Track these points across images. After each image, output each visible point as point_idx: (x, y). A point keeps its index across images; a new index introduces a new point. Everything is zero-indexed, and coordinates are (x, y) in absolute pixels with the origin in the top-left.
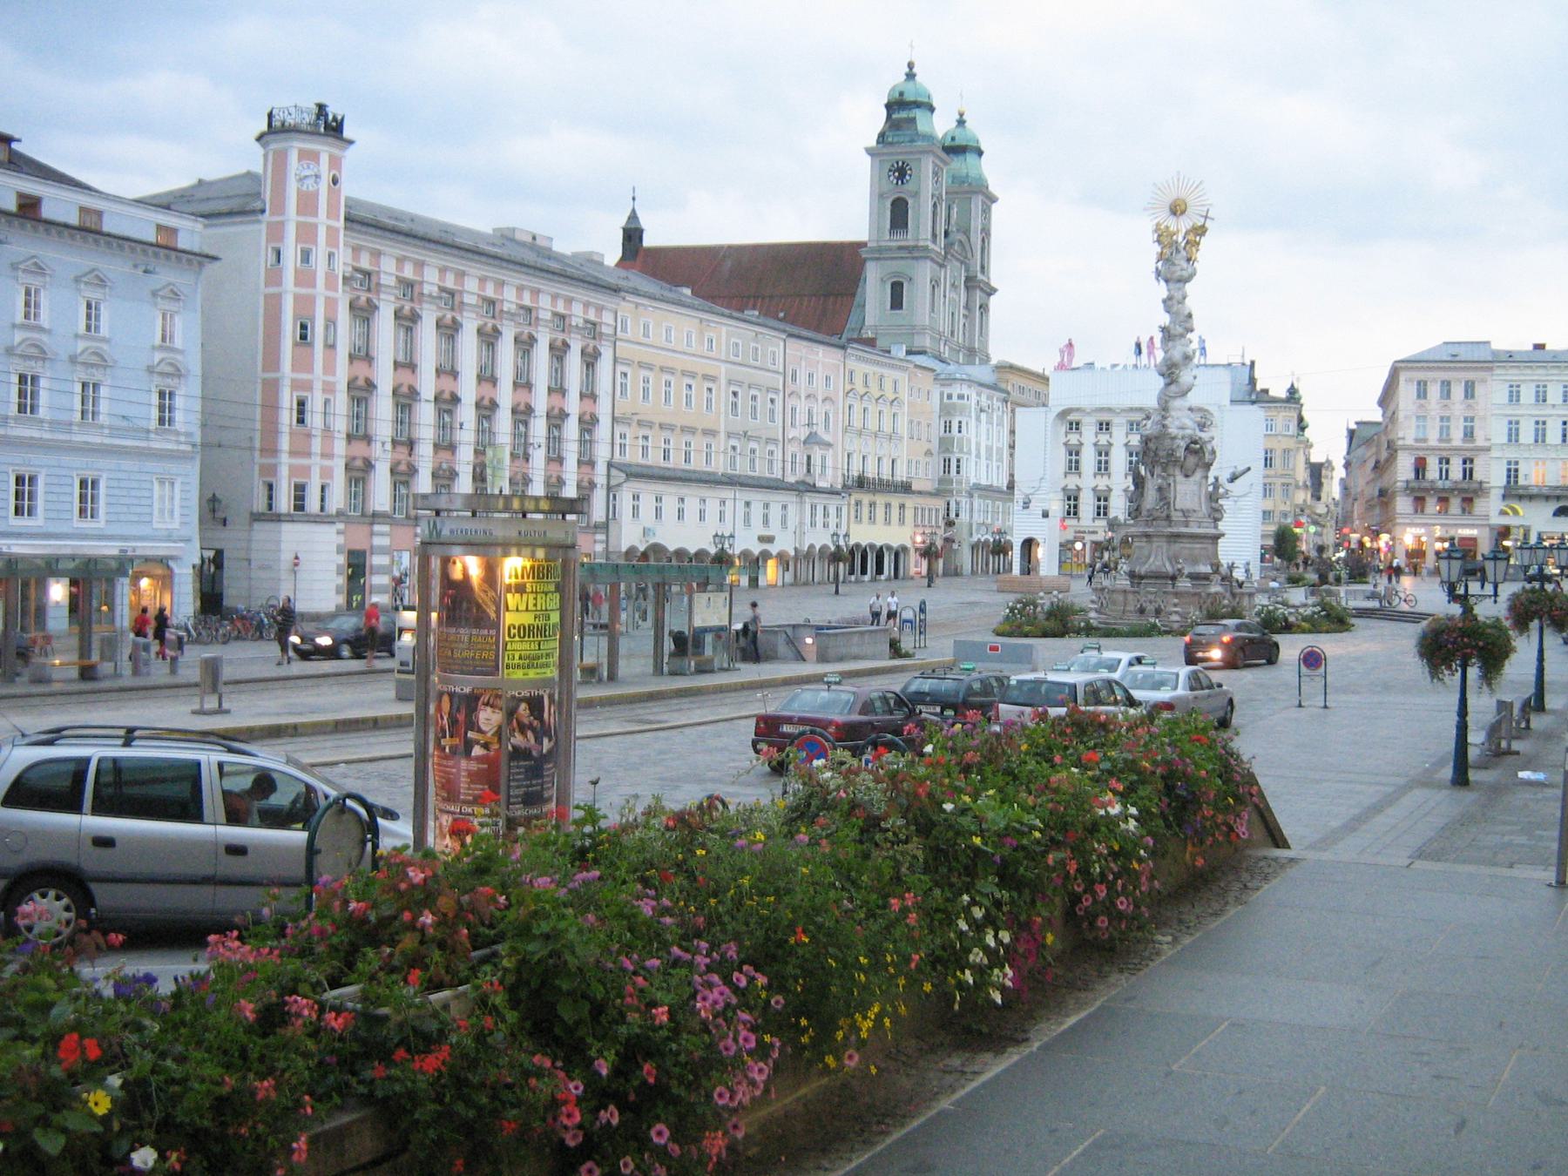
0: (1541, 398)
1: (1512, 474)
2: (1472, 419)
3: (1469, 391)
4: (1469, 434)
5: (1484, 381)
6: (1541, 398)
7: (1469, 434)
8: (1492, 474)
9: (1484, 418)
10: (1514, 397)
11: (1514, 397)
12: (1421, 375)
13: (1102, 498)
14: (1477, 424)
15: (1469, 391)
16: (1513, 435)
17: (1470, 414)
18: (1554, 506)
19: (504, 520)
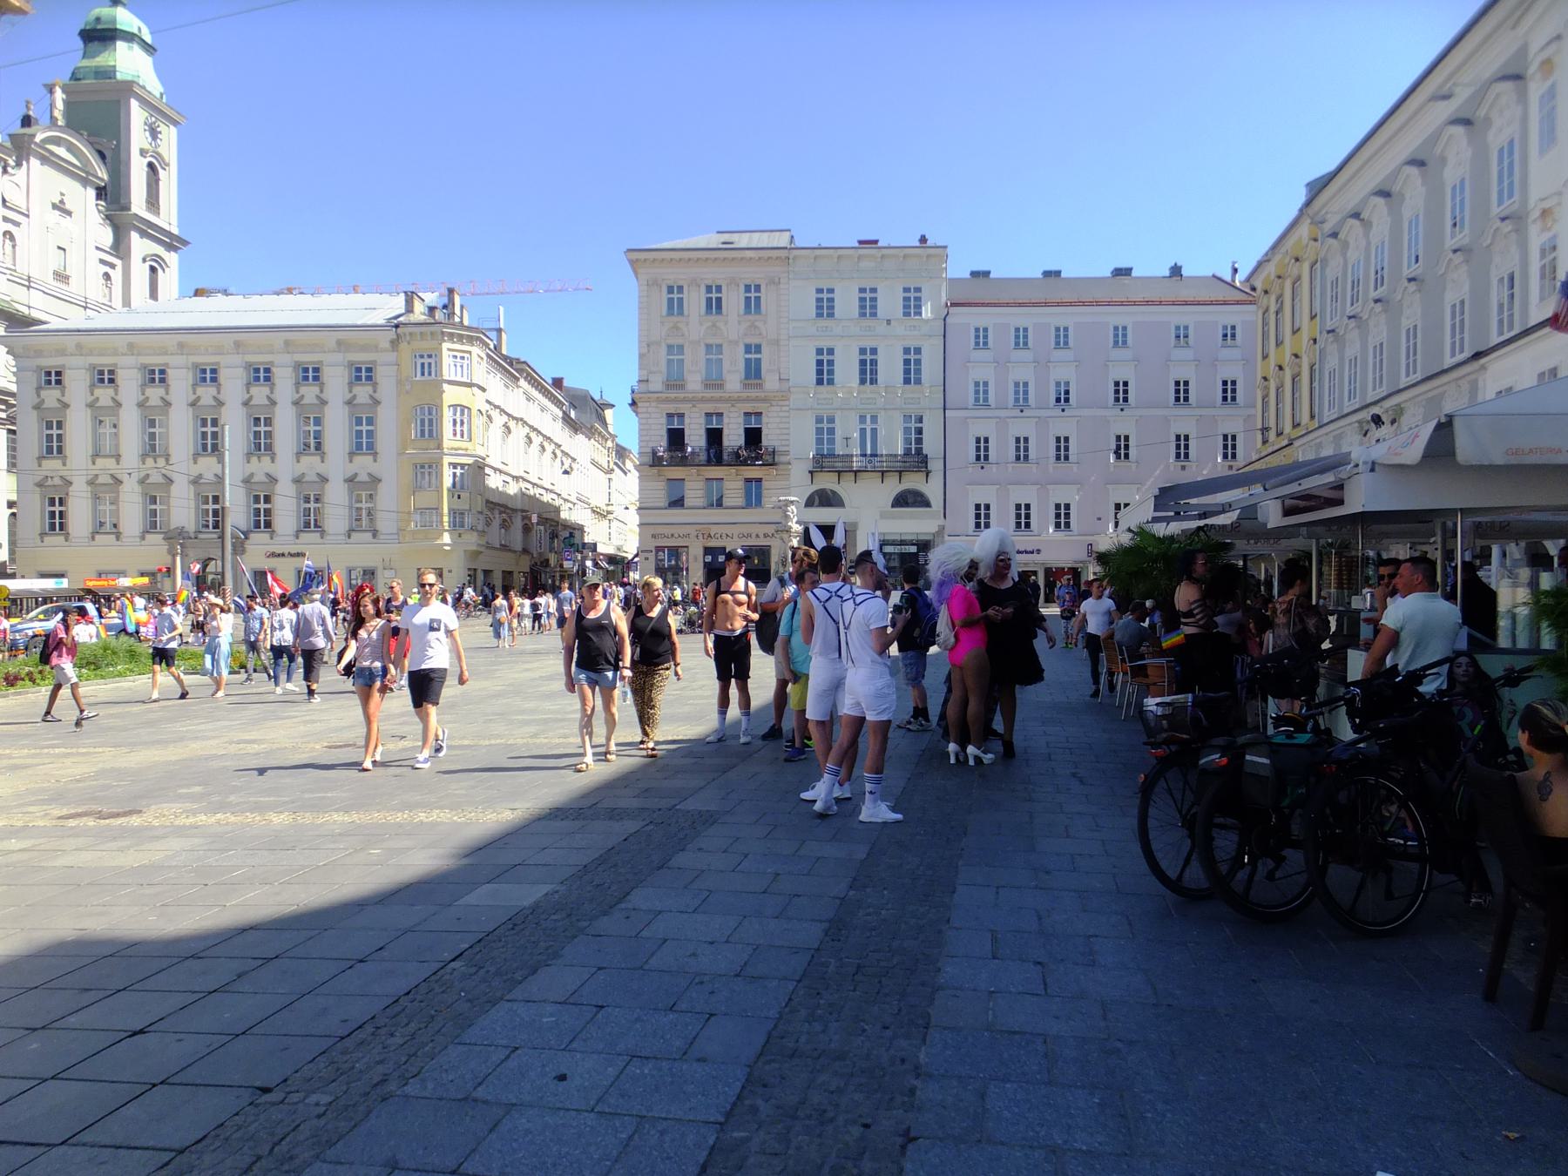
0: (868, 306)
1: (825, 429)
2: (758, 349)
3: (752, 305)
4: (753, 372)
5: (774, 282)
6: (868, 306)
7: (753, 372)
8: (794, 435)
9: (777, 342)
10: (825, 307)
11: (825, 307)
12: (673, 275)
13: (153, 497)
14: (765, 356)
15: (752, 305)
16: (824, 373)
17: (753, 340)
18: (893, 487)
19: (123, 573)
